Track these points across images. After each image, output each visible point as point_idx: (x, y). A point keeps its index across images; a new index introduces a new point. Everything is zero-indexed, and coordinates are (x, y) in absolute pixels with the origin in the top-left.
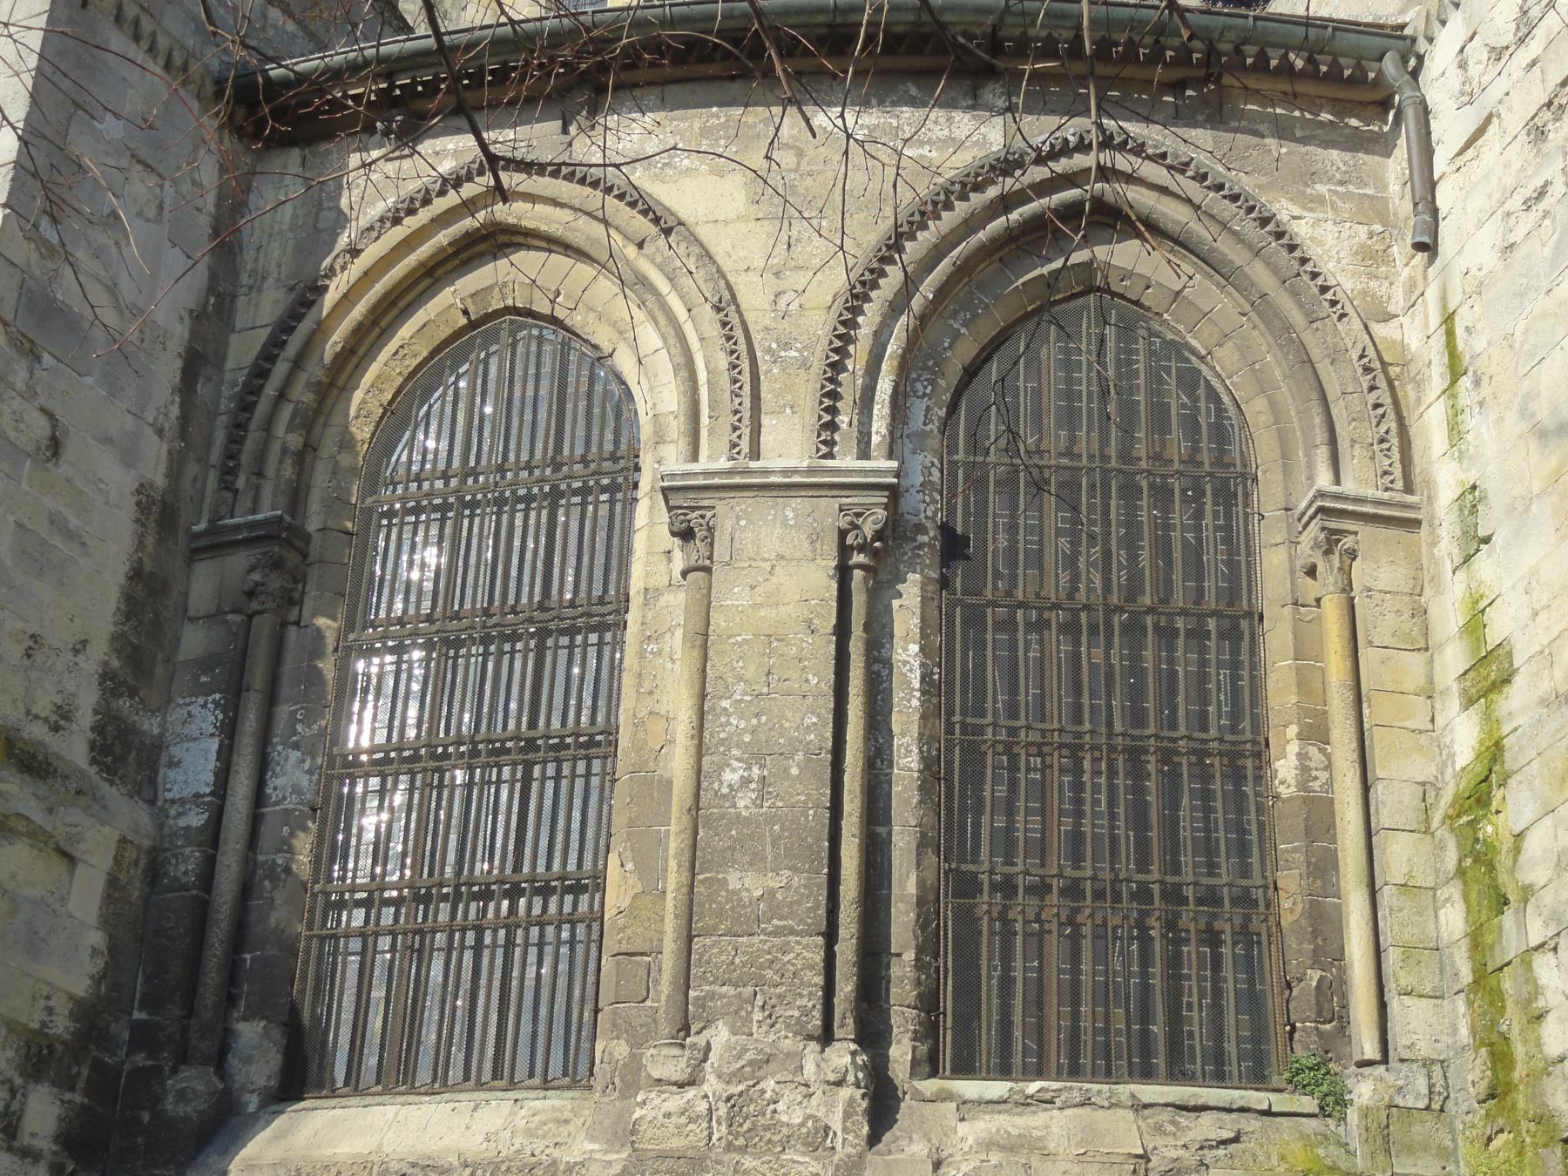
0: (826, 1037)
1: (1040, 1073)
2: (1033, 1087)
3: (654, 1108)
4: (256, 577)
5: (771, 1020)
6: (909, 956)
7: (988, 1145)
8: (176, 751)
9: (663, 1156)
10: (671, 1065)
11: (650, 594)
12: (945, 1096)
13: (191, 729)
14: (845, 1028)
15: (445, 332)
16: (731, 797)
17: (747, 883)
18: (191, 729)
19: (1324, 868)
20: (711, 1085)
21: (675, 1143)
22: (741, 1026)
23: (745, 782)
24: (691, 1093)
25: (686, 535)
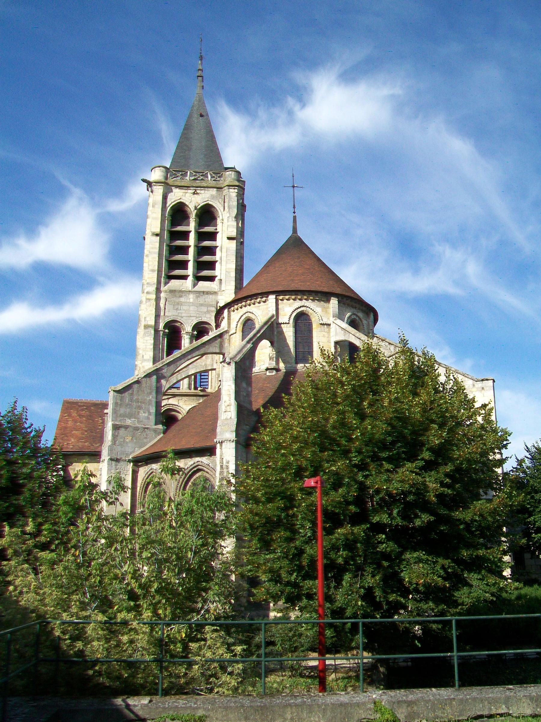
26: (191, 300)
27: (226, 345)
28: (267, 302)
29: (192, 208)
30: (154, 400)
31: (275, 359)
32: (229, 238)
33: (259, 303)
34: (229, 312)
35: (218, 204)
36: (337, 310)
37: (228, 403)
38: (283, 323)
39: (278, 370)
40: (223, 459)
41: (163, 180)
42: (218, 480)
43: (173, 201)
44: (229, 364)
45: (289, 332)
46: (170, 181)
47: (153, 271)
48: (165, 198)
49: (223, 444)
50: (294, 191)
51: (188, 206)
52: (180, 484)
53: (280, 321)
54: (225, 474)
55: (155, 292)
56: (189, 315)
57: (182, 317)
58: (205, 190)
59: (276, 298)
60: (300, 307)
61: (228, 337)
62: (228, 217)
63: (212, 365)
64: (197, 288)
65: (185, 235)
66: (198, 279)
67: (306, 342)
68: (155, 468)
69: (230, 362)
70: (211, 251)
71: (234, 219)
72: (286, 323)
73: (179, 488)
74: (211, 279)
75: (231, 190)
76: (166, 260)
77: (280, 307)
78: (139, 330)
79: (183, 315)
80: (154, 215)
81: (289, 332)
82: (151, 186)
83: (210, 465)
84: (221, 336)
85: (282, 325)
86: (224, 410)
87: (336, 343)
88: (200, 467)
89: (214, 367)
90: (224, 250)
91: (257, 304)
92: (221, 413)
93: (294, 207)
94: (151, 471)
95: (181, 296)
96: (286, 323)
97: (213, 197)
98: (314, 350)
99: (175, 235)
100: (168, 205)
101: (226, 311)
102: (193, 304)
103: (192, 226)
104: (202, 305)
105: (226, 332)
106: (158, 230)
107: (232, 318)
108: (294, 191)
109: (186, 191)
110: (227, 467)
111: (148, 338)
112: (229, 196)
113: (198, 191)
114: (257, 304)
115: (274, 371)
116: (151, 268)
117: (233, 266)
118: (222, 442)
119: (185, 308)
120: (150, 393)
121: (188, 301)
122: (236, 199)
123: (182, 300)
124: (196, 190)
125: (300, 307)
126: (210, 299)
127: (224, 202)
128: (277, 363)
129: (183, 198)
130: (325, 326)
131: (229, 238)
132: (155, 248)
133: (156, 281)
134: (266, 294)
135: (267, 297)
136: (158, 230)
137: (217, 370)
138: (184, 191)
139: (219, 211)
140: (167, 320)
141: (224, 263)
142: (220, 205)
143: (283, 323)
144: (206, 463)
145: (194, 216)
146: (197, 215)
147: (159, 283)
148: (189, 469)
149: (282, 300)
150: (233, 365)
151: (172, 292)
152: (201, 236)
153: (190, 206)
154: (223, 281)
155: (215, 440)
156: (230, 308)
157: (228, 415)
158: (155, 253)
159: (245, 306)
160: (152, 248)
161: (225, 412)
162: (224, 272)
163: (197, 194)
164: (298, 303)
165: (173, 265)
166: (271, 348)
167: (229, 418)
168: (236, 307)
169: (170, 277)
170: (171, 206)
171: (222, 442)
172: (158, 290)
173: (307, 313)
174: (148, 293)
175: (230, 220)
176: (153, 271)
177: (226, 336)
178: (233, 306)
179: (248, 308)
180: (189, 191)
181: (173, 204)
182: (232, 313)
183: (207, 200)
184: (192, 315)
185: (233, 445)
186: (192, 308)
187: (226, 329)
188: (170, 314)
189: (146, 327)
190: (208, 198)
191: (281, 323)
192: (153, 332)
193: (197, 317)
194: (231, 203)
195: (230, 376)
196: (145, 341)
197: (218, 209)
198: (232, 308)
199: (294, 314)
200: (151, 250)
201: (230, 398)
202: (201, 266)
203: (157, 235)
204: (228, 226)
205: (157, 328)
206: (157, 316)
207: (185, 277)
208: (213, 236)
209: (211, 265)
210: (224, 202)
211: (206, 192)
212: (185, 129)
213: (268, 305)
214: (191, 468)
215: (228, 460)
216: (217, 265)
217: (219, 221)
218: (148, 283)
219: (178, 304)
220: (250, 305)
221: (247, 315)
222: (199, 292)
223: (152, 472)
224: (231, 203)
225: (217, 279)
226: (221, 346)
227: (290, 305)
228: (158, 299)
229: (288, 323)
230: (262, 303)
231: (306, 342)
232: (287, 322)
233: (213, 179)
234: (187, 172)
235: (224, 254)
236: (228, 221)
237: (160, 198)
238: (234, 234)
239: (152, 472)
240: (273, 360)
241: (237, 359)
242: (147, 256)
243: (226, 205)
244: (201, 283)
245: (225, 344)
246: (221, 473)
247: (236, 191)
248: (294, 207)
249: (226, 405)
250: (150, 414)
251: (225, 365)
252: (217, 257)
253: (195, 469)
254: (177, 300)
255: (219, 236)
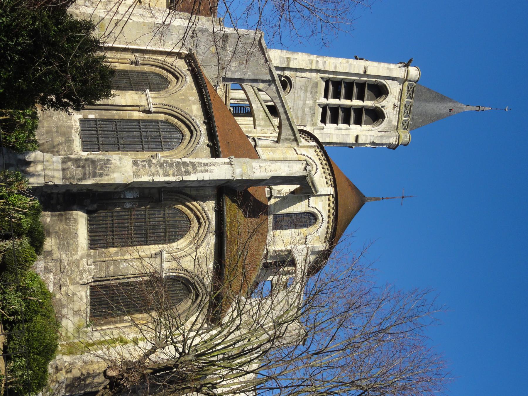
0: (93, 278)
1: (91, 299)
2: (89, 298)
3: (84, 261)
4: (155, 198)
5: (95, 272)
6: (104, 283)
7: (81, 296)
8: (132, 192)
9: (79, 263)
10: (90, 262)
11: (149, 249)
12: (87, 289)
13: (134, 193)
14: (94, 280)
15: (188, 216)
16: (122, 265)
17: (111, 268)
18: (134, 193)
19: (116, 322)
20: (88, 267)
21: (80, 264)
22: (94, 269)
23: (124, 266)
24: (86, 265)
25: (156, 254)
26: (307, 102)
27: (286, 145)
28: (326, 185)
29: (384, 103)
30: (246, 77)
31: (279, 195)
32: (357, 137)
33: (326, 178)
34: (314, 147)
35: (384, 126)
36: (317, 250)
37: (269, 169)
38: (309, 202)
39: (270, 198)
40: (214, 165)
41: (408, 78)
42: (192, 160)
43: (390, 86)
44: (305, 169)
45: (300, 207)
46: (407, 84)
47: (335, 67)
48: (393, 79)
49: (229, 165)
50: (399, 197)
51: (384, 99)
52: (175, 110)
53: (311, 199)
54: (199, 169)
55: (317, 68)
56: (296, 100)
57: (294, 93)
58: (396, 115)
59: (331, 194)
60: (322, 217)
61: (292, 146)
62: (374, 136)
63: (260, 126)
64: (317, 106)
65: (361, 97)
66: (325, 108)
67: (291, 223)
68: (187, 80)
69: (307, 170)
70: (347, 121)
71: (372, 141)
72: (309, 204)
73: (171, 108)
74: (323, 121)
75: (395, 138)
76: (343, 79)
77: (323, 197)
78: (285, 52)
79: (296, 94)
80: (381, 69)
81: (300, 207)
82: (405, 66)
83: (199, 145)
84: (296, 140)
85: (307, 200)
86: (261, 165)
87: (290, 252)
88: (195, 133)
89: (257, 128)
90: (347, 132)
91: (324, 175)
92: (258, 162)
93: (387, 198)
94: (182, 75)
95: (311, 92)
96: (309, 204)
97: (390, 122)
98: (284, 231)
99: (361, 86)
100: (387, 81)
101: (314, 144)
102: (304, 104)
103: (368, 103)
104: (303, 111)
105: (298, 144)
106: (368, 73)
107: (309, 149)
108: (399, 197)
109: (397, 98)
110: (206, 171)
111: (278, 61)
112: (390, 137)
113: (395, 109)
114: (324, 175)
115: (269, 196)
116: (338, 65)
117: (334, 141)
118: (231, 164)
119: (302, 95)
120: (254, 74)
121: (307, 99)
122: (388, 142)
123: (309, 95)
124: (396, 107)
125: (322, 217)
126: (308, 119)
127: (385, 132)
128: (275, 197)
129: (392, 96)
130: (304, 240)
131: (357, 137)
132: (354, 70)
133: (327, 70)
134: (335, 187)
135: (332, 186)
136: (368, 73)
137: (255, 130)
138: (397, 96)
139: (378, 127)
140: (292, 79)
141: (337, 132)
142: (383, 128)
143: (309, 202)
144: (200, 141)
145: (376, 105)
146: (377, 107)
147: (325, 72)
148: (192, 121)
149: (329, 200)
150: (304, 173)
151: (316, 85)
152: (359, 111)
153: (385, 101)
154: (322, 131)
155: (233, 157)
156: (318, 148)
157: (257, 170)
158: (350, 69)
159: (321, 164)
160: (354, 67)
161: (260, 167)
162: (329, 132)
163: (394, 108)
164: (325, 214)
165: (337, 84)
166: (288, 191)
167: (254, 170)
168: (320, 154)
169: (327, 82)
170: (386, 84)
171: (231, 164)
172: (318, 71)
173: (317, 223)
174: (317, 62)
175: (372, 138)
176: (335, 67)
177: (294, 144)
178: (320, 151)
179: (320, 166)
180: (397, 101)
181: (388, 87)
182: (313, 150)
183: (388, 117)
184: (295, 103)
185: (229, 177)
186: (301, 103)
187: (300, 145)
188: (297, 82)
189: (288, 59)
190: (390, 118)
191: (309, 200)
192: (284, 66)
193: (293, 107)
194: (385, 138)
195: (294, 171)
196: (276, 58)
197: (380, 126)
198: (318, 150)
199: (316, 212)
200: (353, 66)
201: (273, 171)
202: (335, 110)
203: (365, 72)
204: (367, 135)
205: (286, 69)
206: (296, 70)
207: (326, 96)
208: (358, 122)
209: (334, 121)
210: (385, 132)
211: (395, 116)
212: (442, 96)
213: (324, 187)
214: (193, 123)
215: (213, 171)
216: (335, 125)
217: (369, 127)
218: (325, 62)
219: (306, 90)
220: (323, 168)
221: (314, 165)
222: (314, 109)
223: (182, 77)
224: (385, 138)
225: (323, 125)
226: (287, 140)
227: (324, 208)
228: (311, 71)
229: (309, 207)
230: (325, 180)
231: (291, 223)
232: (310, 206)
233: (404, 122)
234: (411, 99)
235: (343, 132)
236: (370, 135)
237: (394, 75)
238: (360, 141)
239: (182, 77)
240: (278, 193)
241: (308, 179)
242: (348, 62)
243: (383, 134)
244: (320, 110)
245: (287, 143)
246: (200, 164)
247: (394, 143)
248: (387, 198)
249: (267, 167)
250: (234, 72)
251: (304, 166)
252: (341, 126)
253: (192, 128)
254: (309, 89)
255: (358, 126)
